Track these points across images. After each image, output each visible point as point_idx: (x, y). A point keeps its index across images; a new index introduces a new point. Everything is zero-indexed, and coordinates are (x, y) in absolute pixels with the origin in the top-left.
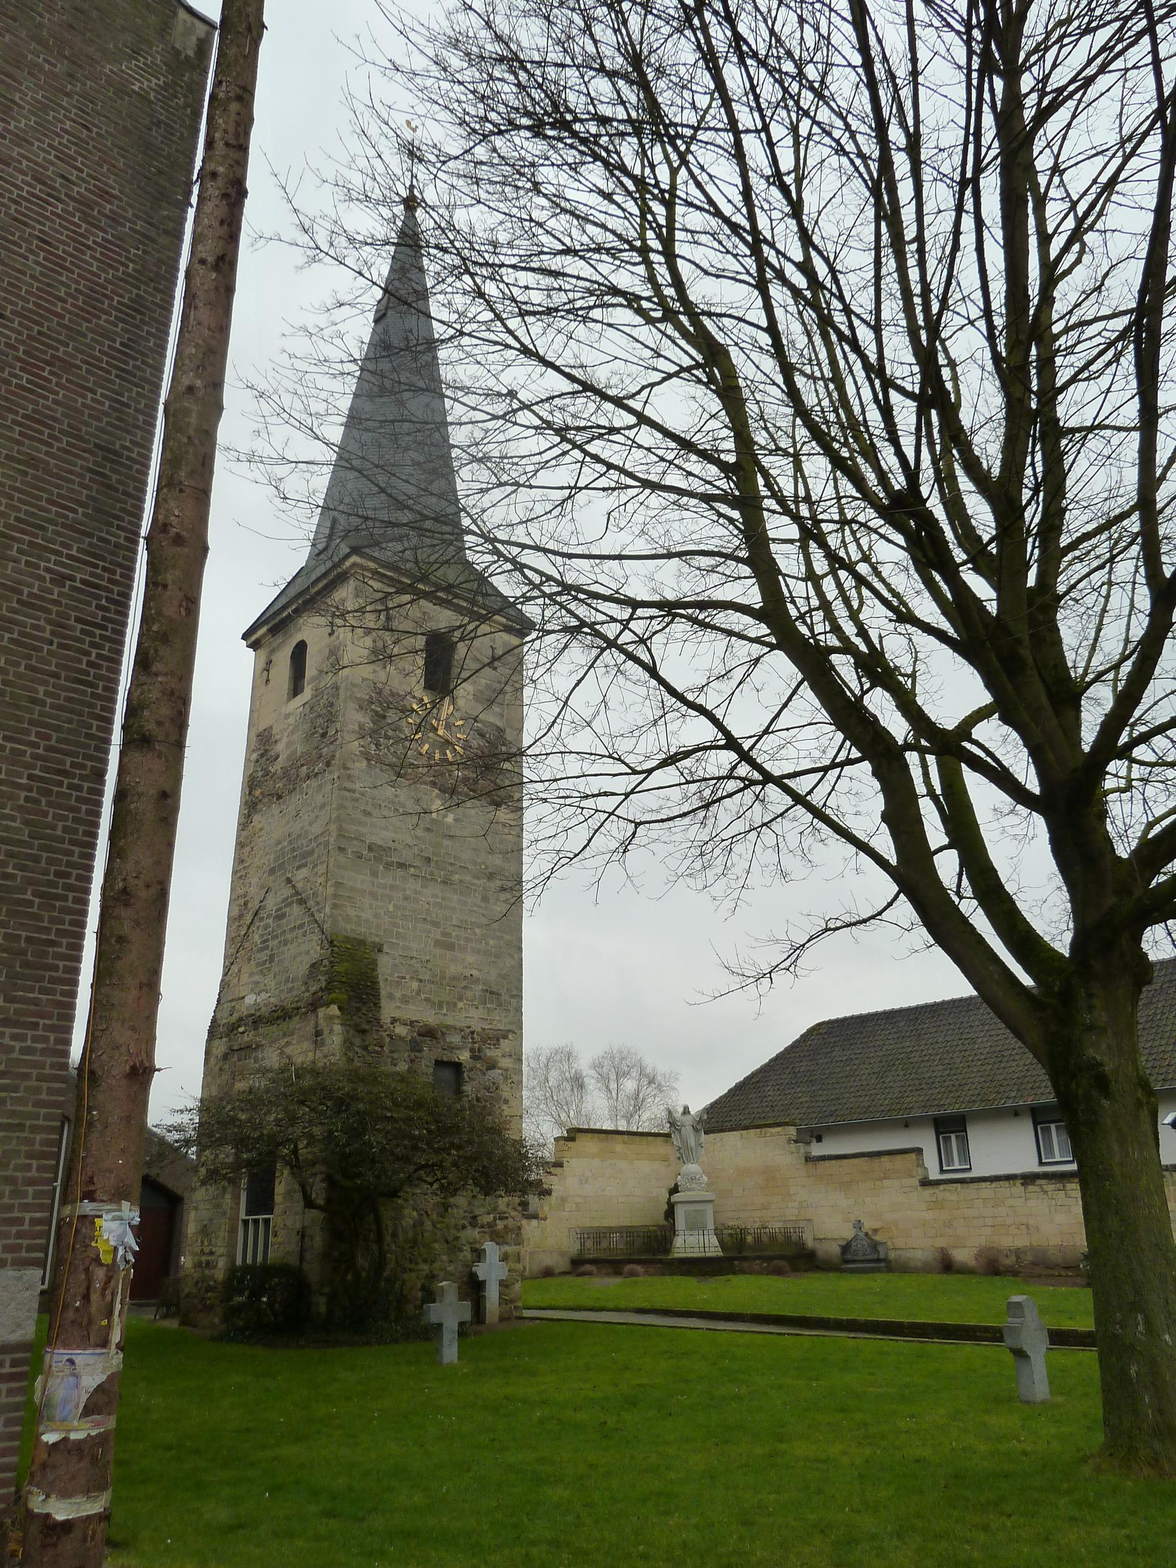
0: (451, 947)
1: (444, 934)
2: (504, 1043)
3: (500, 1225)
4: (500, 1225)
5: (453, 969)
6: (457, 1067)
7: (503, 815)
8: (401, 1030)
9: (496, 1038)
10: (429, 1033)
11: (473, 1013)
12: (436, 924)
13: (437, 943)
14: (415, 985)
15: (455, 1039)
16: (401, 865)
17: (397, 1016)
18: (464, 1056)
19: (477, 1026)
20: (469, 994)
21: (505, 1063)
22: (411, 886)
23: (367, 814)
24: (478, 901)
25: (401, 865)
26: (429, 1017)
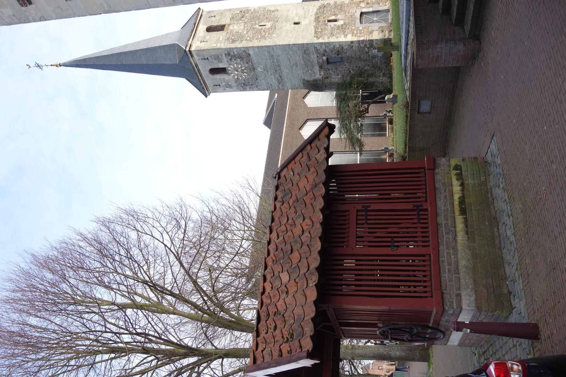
0: (296, 63)
1: (294, 65)
2: (318, 48)
3: (368, 46)
4: (368, 46)
5: (302, 62)
6: (327, 59)
7: (251, 52)
8: (322, 73)
9: (317, 50)
10: (321, 67)
11: (312, 56)
12: (292, 68)
13: (297, 67)
14: (310, 71)
15: (321, 60)
16: (280, 77)
17: (318, 74)
18: (325, 58)
19: (315, 56)
20: (307, 58)
21: (324, 47)
22: (284, 73)
23: (271, 85)
24: (281, 57)
25: (280, 77)
26: (317, 68)
